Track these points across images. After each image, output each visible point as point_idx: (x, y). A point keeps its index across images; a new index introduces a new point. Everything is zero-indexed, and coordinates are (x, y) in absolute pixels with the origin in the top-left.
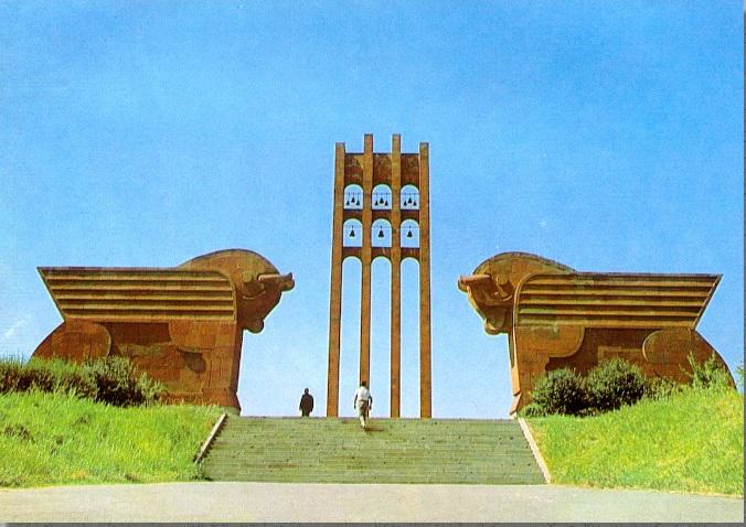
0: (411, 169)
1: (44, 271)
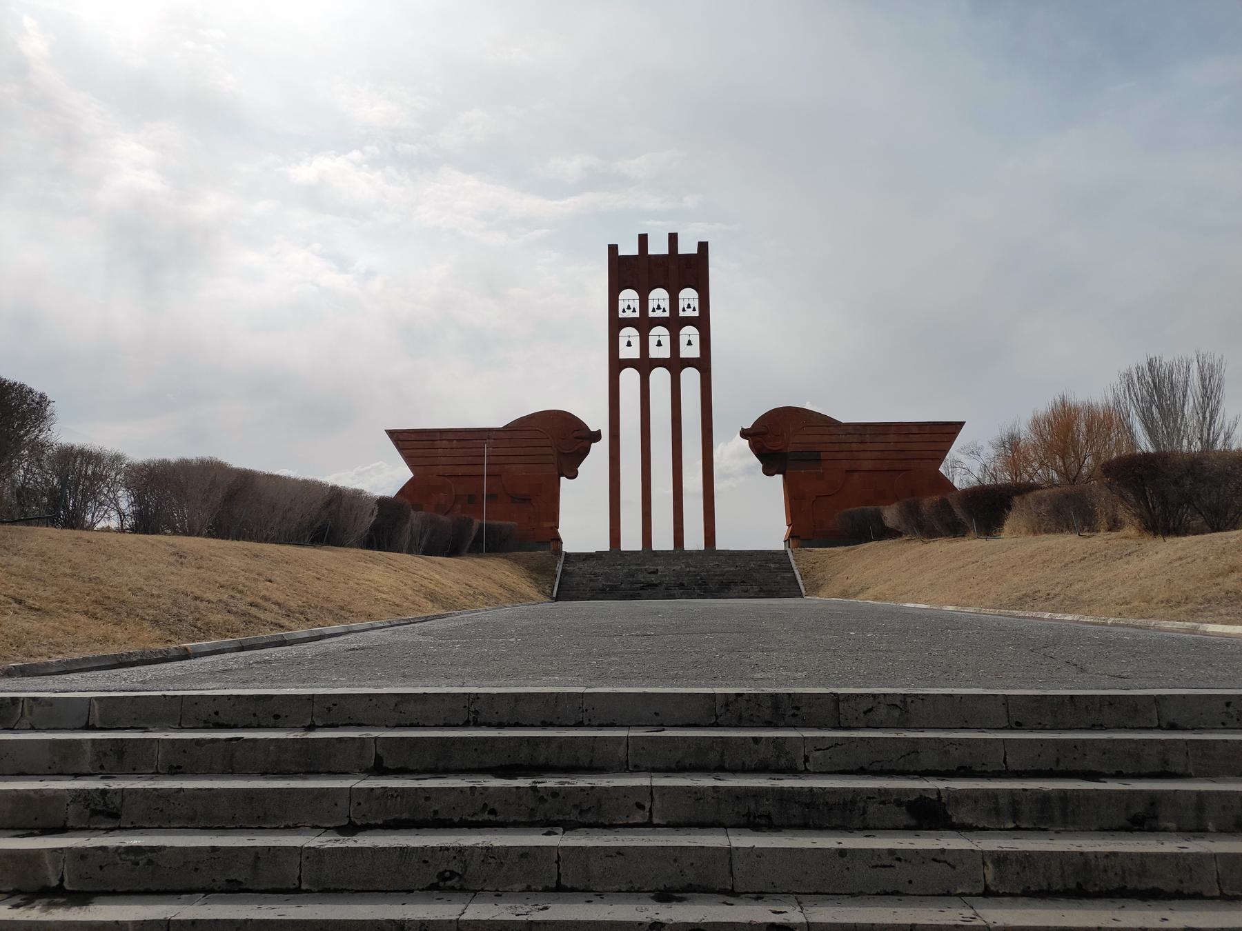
0: (688, 269)
1: (392, 434)
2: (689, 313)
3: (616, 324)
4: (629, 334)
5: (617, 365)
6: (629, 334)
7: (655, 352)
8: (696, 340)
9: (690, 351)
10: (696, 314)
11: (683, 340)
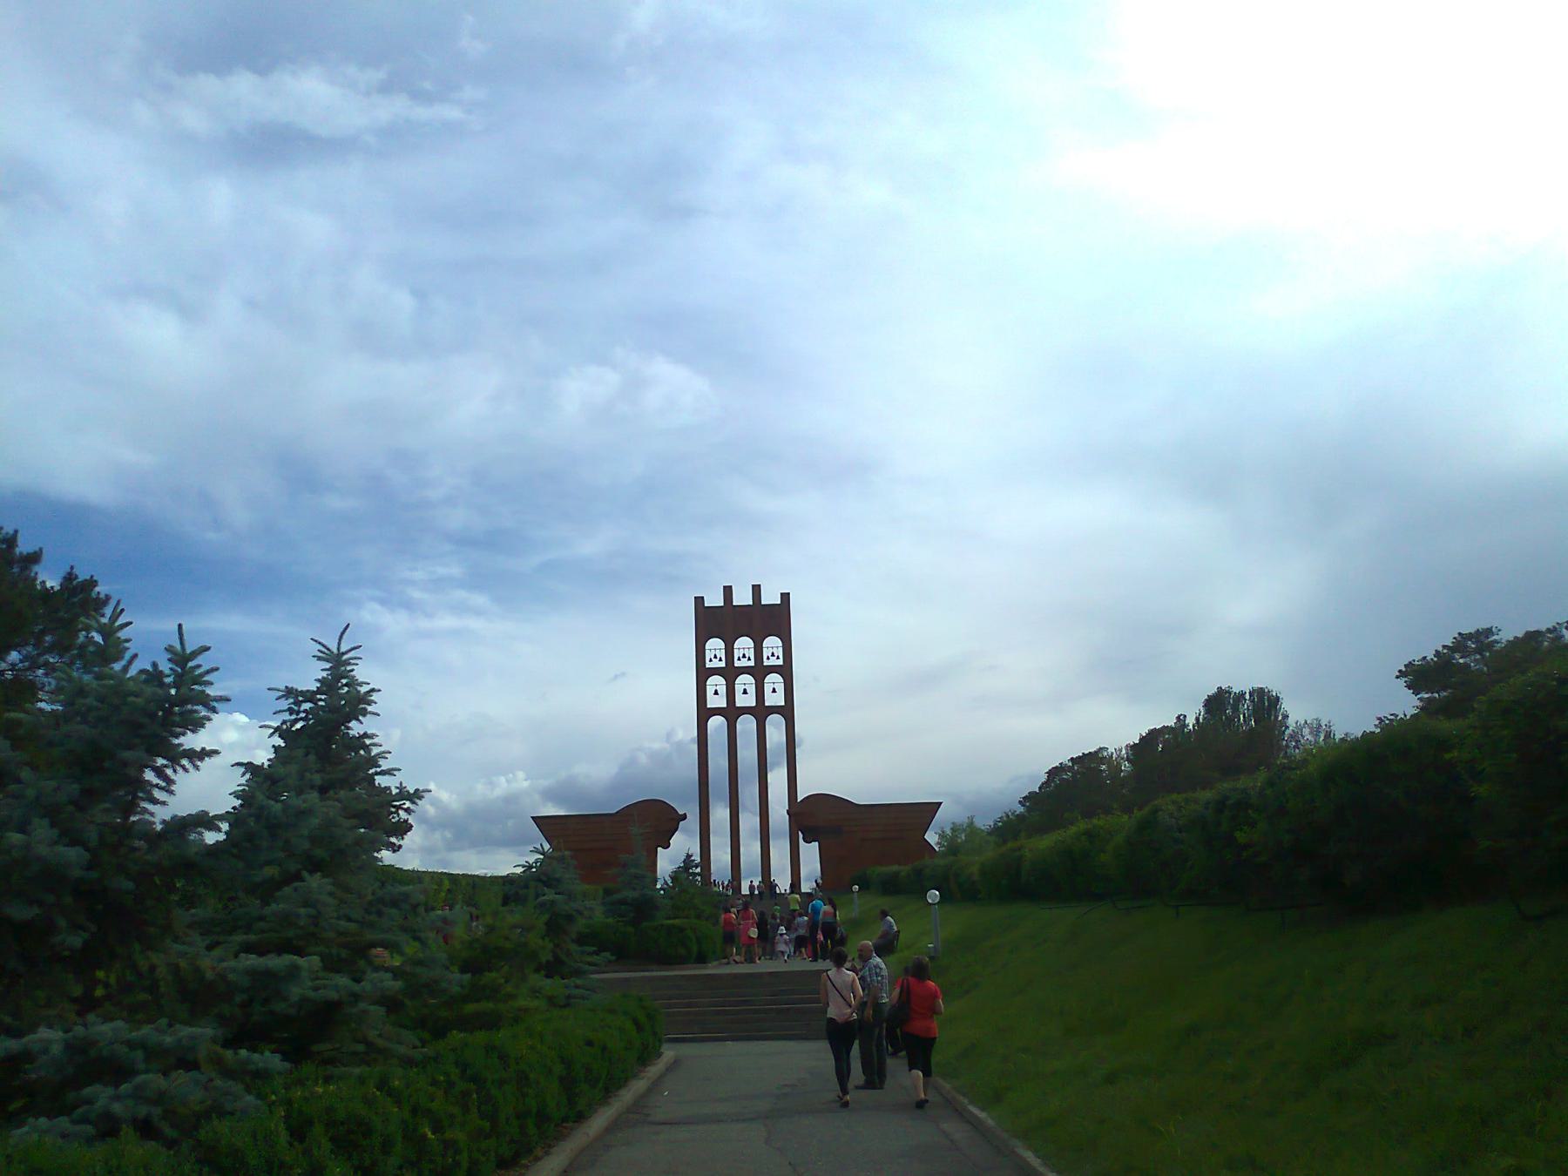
0: (771, 619)
2: (773, 662)
3: (703, 673)
4: (716, 683)
5: (704, 713)
6: (716, 683)
7: (743, 701)
8: (781, 688)
9: (775, 699)
10: (780, 662)
11: (768, 689)
